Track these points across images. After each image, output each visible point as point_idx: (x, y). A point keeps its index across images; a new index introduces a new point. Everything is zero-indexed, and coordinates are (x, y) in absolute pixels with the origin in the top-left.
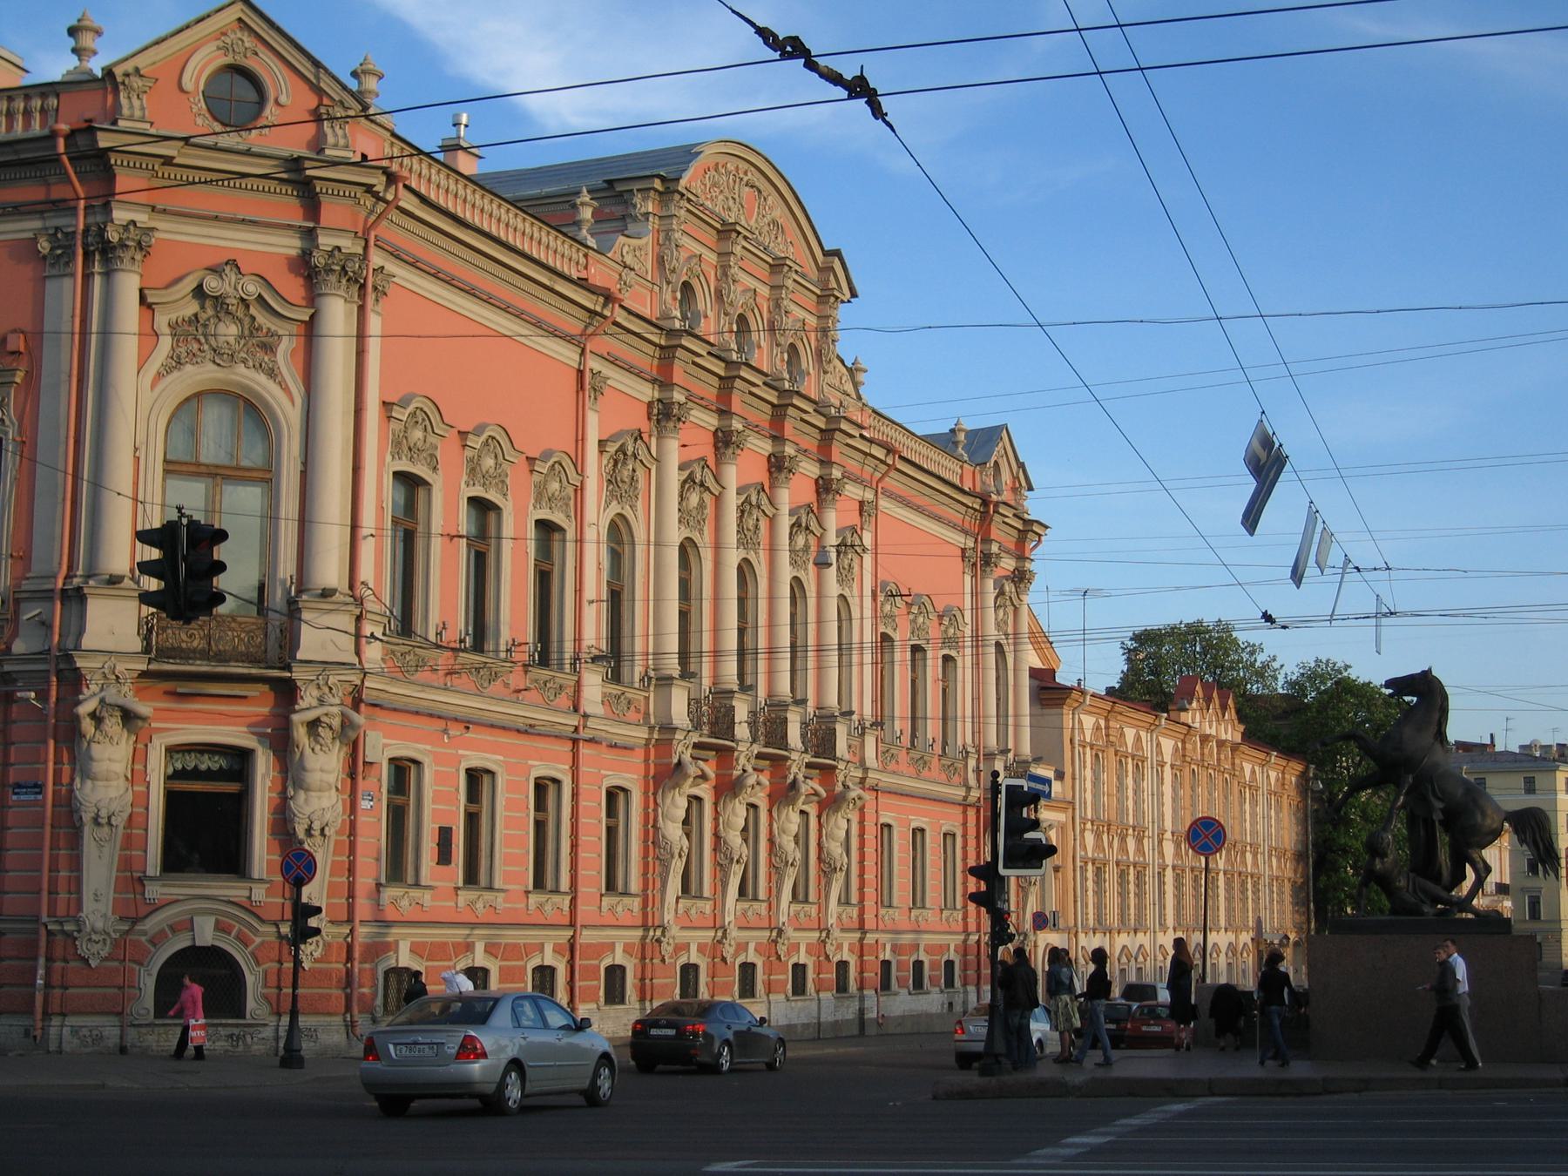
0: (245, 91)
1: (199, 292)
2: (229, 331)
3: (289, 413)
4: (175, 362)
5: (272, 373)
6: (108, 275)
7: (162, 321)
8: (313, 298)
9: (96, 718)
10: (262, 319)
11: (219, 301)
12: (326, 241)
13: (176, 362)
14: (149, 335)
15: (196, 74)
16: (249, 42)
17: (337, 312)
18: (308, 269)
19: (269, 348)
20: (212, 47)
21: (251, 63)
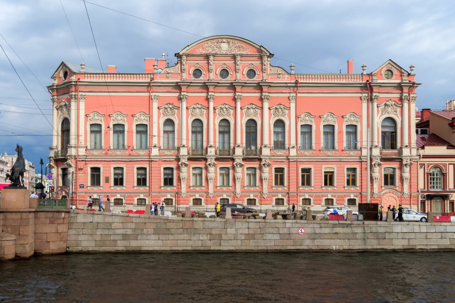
0: (390, 73)
1: (386, 105)
2: (390, 109)
3: (398, 121)
4: (382, 114)
5: (397, 115)
6: (372, 103)
7: (380, 109)
8: (402, 104)
9: (375, 165)
10: (395, 107)
11: (388, 105)
12: (404, 95)
13: (382, 114)
14: (378, 111)
15: (383, 72)
16: (391, 66)
17: (406, 105)
18: (401, 99)
19: (396, 111)
20: (385, 68)
21: (391, 69)
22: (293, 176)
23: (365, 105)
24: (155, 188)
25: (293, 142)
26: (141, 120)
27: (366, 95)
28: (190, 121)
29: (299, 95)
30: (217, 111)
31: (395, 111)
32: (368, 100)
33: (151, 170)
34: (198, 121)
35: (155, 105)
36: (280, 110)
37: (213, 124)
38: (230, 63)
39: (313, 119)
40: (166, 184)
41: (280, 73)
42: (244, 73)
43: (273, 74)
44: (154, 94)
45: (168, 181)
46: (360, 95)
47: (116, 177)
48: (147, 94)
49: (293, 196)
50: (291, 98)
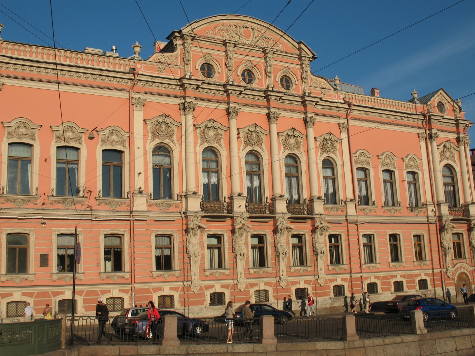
1: (445, 146)
2: (448, 154)
3: (458, 169)
4: (441, 160)
5: (454, 161)
10: (452, 150)
19: (453, 157)
22: (352, 248)
23: (423, 145)
24: (140, 274)
25: (350, 195)
26: (113, 142)
27: (423, 131)
28: (200, 150)
29: (352, 122)
30: (241, 135)
31: (452, 156)
32: (426, 139)
33: (132, 240)
34: (210, 150)
35: (139, 116)
36: (329, 142)
37: (235, 158)
38: (258, 60)
39: (370, 159)
40: (159, 267)
41: (324, 87)
42: (277, 80)
43: (315, 87)
44: (137, 96)
45: (164, 263)
46: (417, 131)
47: (62, 252)
48: (125, 95)
49: (356, 279)
50: (341, 125)
